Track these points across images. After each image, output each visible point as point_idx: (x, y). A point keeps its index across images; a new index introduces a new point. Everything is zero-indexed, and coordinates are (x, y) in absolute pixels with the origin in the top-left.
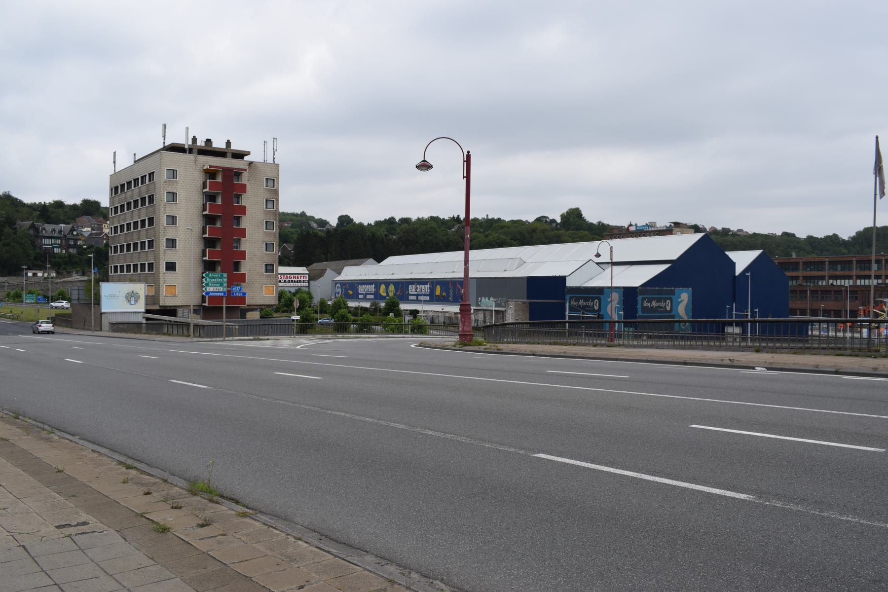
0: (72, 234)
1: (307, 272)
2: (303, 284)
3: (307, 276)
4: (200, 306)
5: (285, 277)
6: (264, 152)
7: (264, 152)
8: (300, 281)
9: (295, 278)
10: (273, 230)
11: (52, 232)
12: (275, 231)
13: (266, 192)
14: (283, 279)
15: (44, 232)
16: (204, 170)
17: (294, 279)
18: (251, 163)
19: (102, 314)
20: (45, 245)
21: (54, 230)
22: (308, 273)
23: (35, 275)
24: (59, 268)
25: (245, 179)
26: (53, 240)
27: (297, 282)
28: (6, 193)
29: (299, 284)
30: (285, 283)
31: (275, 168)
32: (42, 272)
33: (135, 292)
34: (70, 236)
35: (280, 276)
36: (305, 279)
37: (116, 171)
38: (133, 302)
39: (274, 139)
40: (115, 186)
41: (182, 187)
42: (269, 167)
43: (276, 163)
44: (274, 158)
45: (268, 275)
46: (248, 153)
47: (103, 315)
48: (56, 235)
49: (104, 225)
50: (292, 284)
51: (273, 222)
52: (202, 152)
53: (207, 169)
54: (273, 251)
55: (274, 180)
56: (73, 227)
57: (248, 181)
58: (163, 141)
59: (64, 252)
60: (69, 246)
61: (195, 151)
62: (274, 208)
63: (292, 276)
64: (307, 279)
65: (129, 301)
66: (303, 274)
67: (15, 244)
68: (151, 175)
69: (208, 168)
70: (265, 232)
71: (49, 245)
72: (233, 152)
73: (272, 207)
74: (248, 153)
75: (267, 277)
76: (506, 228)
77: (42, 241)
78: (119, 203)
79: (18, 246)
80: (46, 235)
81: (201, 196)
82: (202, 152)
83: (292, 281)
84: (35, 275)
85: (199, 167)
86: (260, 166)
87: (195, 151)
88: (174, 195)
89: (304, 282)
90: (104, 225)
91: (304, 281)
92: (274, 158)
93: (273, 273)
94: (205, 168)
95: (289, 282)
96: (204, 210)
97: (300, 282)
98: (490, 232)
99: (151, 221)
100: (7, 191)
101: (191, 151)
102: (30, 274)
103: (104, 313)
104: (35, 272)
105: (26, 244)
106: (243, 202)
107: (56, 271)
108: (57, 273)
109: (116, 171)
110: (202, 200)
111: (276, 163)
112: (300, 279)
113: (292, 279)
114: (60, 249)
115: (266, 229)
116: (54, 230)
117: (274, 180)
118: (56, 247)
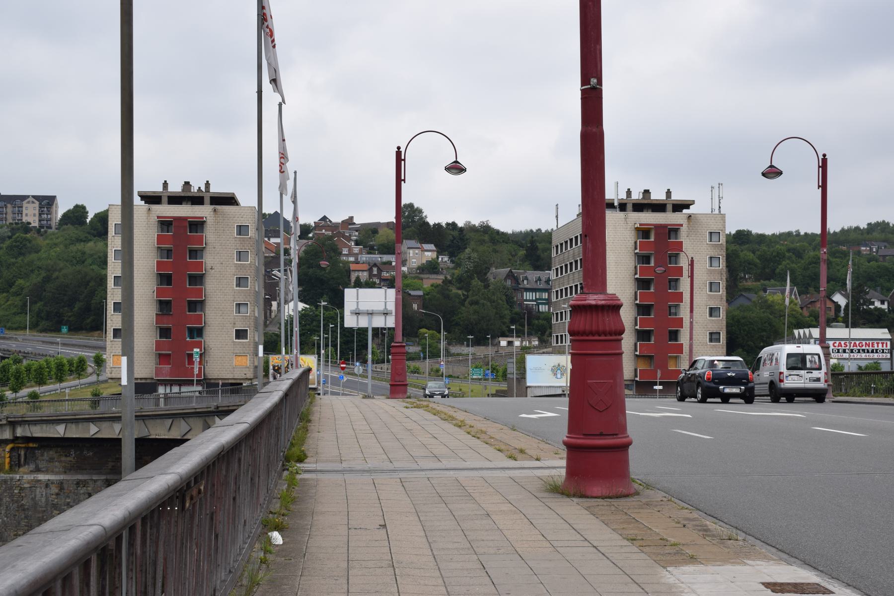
1: (889, 336)
2: (881, 355)
3: (889, 343)
4: (633, 381)
5: (852, 345)
6: (712, 199)
7: (712, 199)
8: (877, 350)
9: (869, 347)
10: (720, 292)
11: (536, 281)
12: (721, 293)
13: (709, 248)
14: (848, 348)
15: (525, 282)
16: (636, 228)
17: (867, 348)
18: (690, 216)
19: (527, 387)
20: (526, 300)
21: (539, 279)
22: (890, 338)
23: (510, 343)
25: (684, 237)
26: (537, 294)
27: (872, 352)
28: (484, 223)
29: (876, 356)
30: (852, 354)
31: (720, 219)
32: (520, 339)
33: (561, 365)
35: (845, 344)
36: (885, 348)
37: (559, 227)
38: (559, 376)
39: (719, 184)
40: (556, 244)
41: (611, 249)
42: (713, 218)
43: (722, 213)
44: (720, 207)
45: (713, 345)
46: (693, 202)
47: (528, 389)
48: (541, 286)
50: (863, 355)
51: (720, 283)
52: (639, 207)
53: (637, 227)
54: (720, 317)
55: (719, 233)
57: (688, 236)
61: (629, 207)
62: (719, 267)
63: (864, 342)
64: (889, 347)
65: (555, 374)
67: (485, 302)
69: (638, 226)
70: (709, 295)
71: (532, 301)
72: (675, 203)
73: (718, 266)
74: (693, 202)
75: (712, 348)
77: (522, 296)
78: (559, 265)
79: (489, 304)
80: (528, 286)
81: (633, 257)
82: (639, 207)
83: (864, 350)
84: (510, 343)
85: (630, 225)
86: (702, 218)
87: (629, 207)
89: (883, 352)
91: (883, 350)
92: (720, 207)
93: (720, 342)
94: (636, 226)
95: (859, 352)
97: (877, 352)
100: (484, 220)
102: (503, 343)
103: (530, 387)
104: (510, 339)
105: (500, 301)
106: (681, 262)
107: (539, 338)
109: (559, 227)
110: (633, 262)
111: (722, 213)
112: (876, 348)
113: (864, 348)
114: (547, 306)
115: (711, 291)
116: (539, 279)
117: (719, 233)
118: (542, 304)
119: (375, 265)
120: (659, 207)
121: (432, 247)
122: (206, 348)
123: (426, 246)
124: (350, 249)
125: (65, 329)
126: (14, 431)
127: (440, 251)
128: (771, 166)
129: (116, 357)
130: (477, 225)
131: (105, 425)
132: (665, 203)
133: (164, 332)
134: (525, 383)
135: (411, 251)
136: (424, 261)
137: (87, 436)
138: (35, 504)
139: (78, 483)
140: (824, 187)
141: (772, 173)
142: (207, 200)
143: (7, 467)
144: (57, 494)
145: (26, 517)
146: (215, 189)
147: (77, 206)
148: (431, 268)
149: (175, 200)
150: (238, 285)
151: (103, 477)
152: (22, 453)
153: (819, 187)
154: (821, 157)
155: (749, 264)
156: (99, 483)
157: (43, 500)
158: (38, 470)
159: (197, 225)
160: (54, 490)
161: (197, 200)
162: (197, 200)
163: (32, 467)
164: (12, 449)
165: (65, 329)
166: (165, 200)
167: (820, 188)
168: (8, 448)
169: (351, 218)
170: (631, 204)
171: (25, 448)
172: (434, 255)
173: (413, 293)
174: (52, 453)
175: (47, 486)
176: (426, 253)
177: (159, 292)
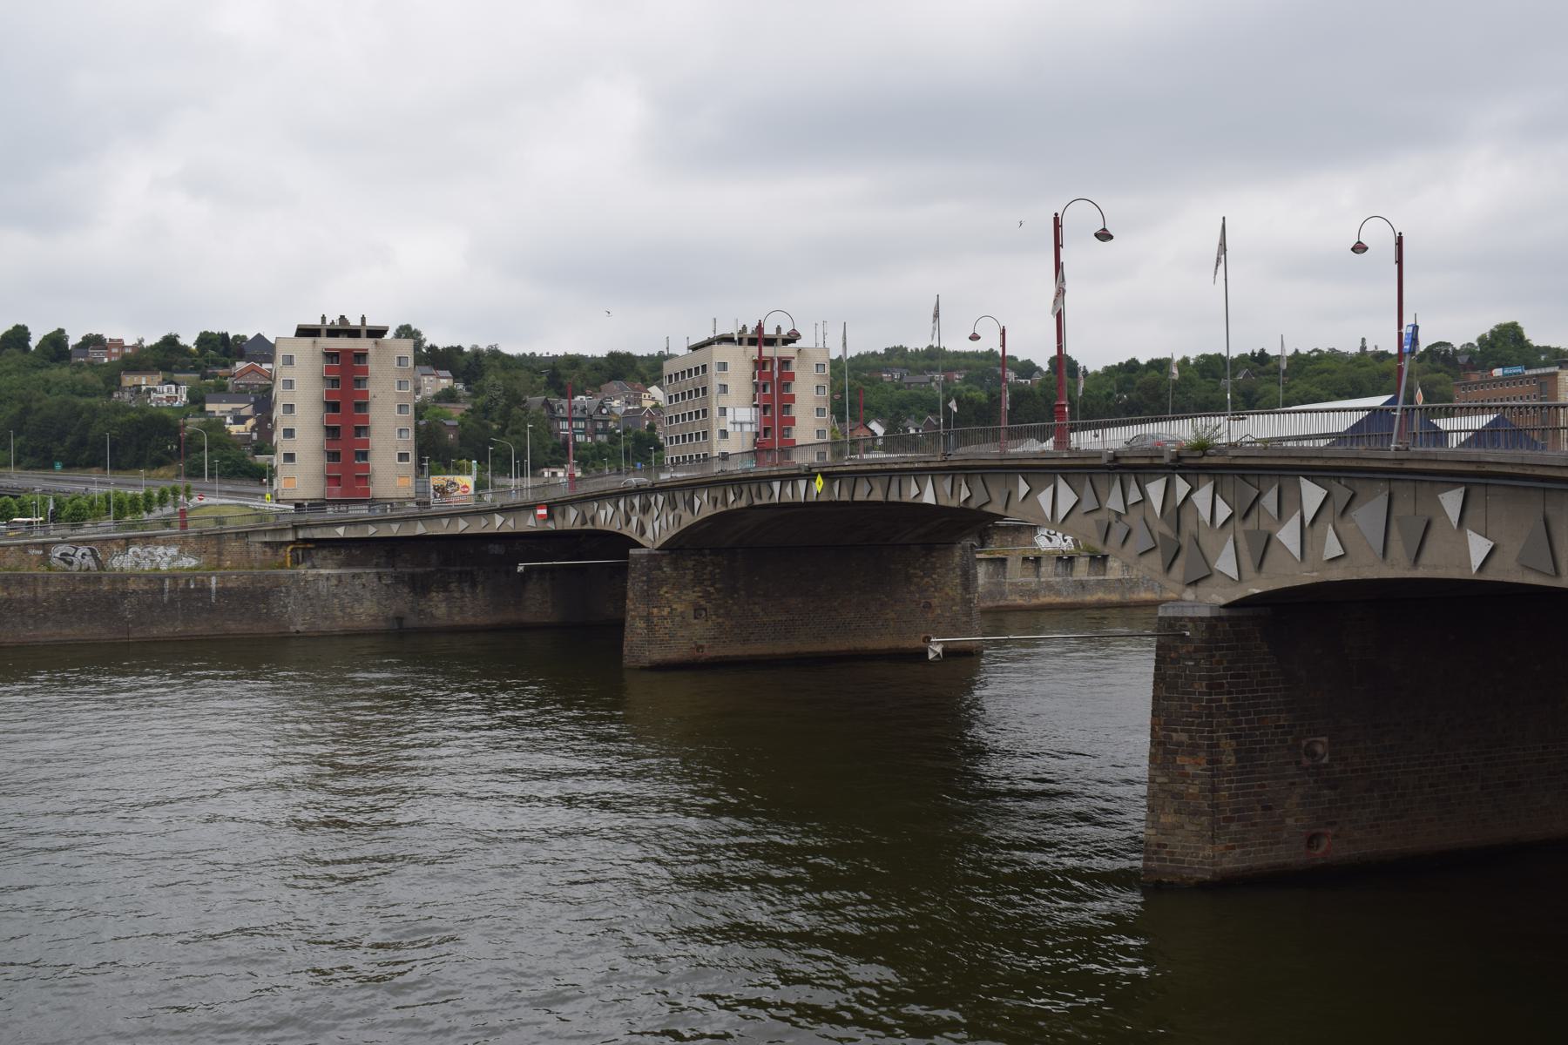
0: (601, 412)
15: (561, 411)
18: (799, 350)
20: (562, 430)
23: (554, 474)
24: (585, 465)
34: (596, 417)
48: (577, 415)
56: (601, 402)
58: (712, 329)
59: (589, 440)
60: (597, 432)
61: (745, 341)
68: (704, 367)
76: (1326, 374)
77: (558, 425)
88: (725, 386)
96: (754, 400)
98: (1297, 381)
99: (705, 411)
100: (493, 343)
101: (740, 341)
104: (554, 470)
108: (583, 471)
118: (579, 434)
120: (771, 342)
121: (447, 373)
123: (441, 373)
125: (58, 466)
126: (296, 533)
127: (456, 378)
130: (485, 348)
131: (382, 526)
133: (333, 456)
135: (426, 378)
136: (440, 389)
137: (365, 536)
138: (318, 595)
139: (354, 576)
142: (364, 333)
143: (289, 565)
144: (337, 586)
145: (311, 605)
147: (17, 327)
148: (448, 396)
149: (333, 333)
150: (400, 412)
151: (374, 571)
152: (300, 553)
156: (371, 575)
157: (325, 590)
158: (314, 567)
159: (361, 356)
160: (334, 582)
161: (354, 333)
163: (309, 564)
164: (292, 550)
165: (58, 466)
166: (324, 332)
168: (289, 549)
171: (304, 549)
172: (451, 381)
173: (448, 423)
174: (325, 552)
175: (328, 579)
176: (442, 381)
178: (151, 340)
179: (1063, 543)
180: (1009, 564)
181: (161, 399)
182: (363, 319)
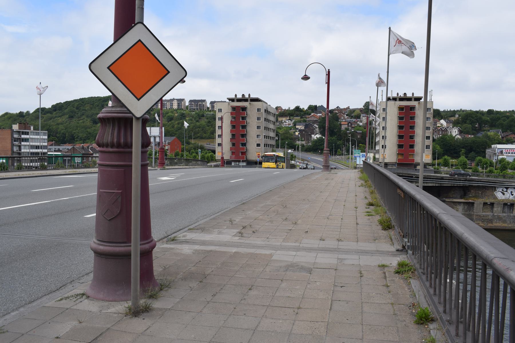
5: (512, 151)
12: (431, 131)
14: (511, 152)
30: (512, 154)
35: (509, 150)
49: (438, 122)
52: (401, 99)
66: (513, 149)
82: (401, 99)
90: (438, 122)
119: (350, 122)
122: (247, 150)
124: (344, 117)
128: (306, 75)
129: (218, 153)
132: (411, 97)
134: (356, 163)
135: (364, 118)
140: (328, 83)
141: (306, 78)
142: (249, 100)
146: (252, 96)
149: (239, 100)
153: (326, 83)
154: (327, 71)
155: (486, 121)
159: (244, 109)
162: (246, 100)
167: (327, 84)
169: (349, 107)
170: (414, 99)
173: (358, 132)
177: (231, 131)
178: (292, 108)
179: (511, 196)
180: (475, 205)
181: (287, 124)
182: (249, 95)
